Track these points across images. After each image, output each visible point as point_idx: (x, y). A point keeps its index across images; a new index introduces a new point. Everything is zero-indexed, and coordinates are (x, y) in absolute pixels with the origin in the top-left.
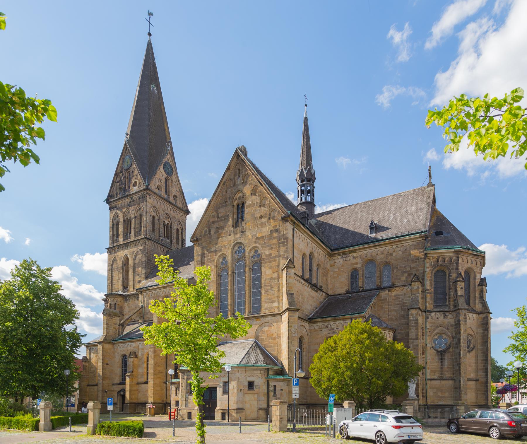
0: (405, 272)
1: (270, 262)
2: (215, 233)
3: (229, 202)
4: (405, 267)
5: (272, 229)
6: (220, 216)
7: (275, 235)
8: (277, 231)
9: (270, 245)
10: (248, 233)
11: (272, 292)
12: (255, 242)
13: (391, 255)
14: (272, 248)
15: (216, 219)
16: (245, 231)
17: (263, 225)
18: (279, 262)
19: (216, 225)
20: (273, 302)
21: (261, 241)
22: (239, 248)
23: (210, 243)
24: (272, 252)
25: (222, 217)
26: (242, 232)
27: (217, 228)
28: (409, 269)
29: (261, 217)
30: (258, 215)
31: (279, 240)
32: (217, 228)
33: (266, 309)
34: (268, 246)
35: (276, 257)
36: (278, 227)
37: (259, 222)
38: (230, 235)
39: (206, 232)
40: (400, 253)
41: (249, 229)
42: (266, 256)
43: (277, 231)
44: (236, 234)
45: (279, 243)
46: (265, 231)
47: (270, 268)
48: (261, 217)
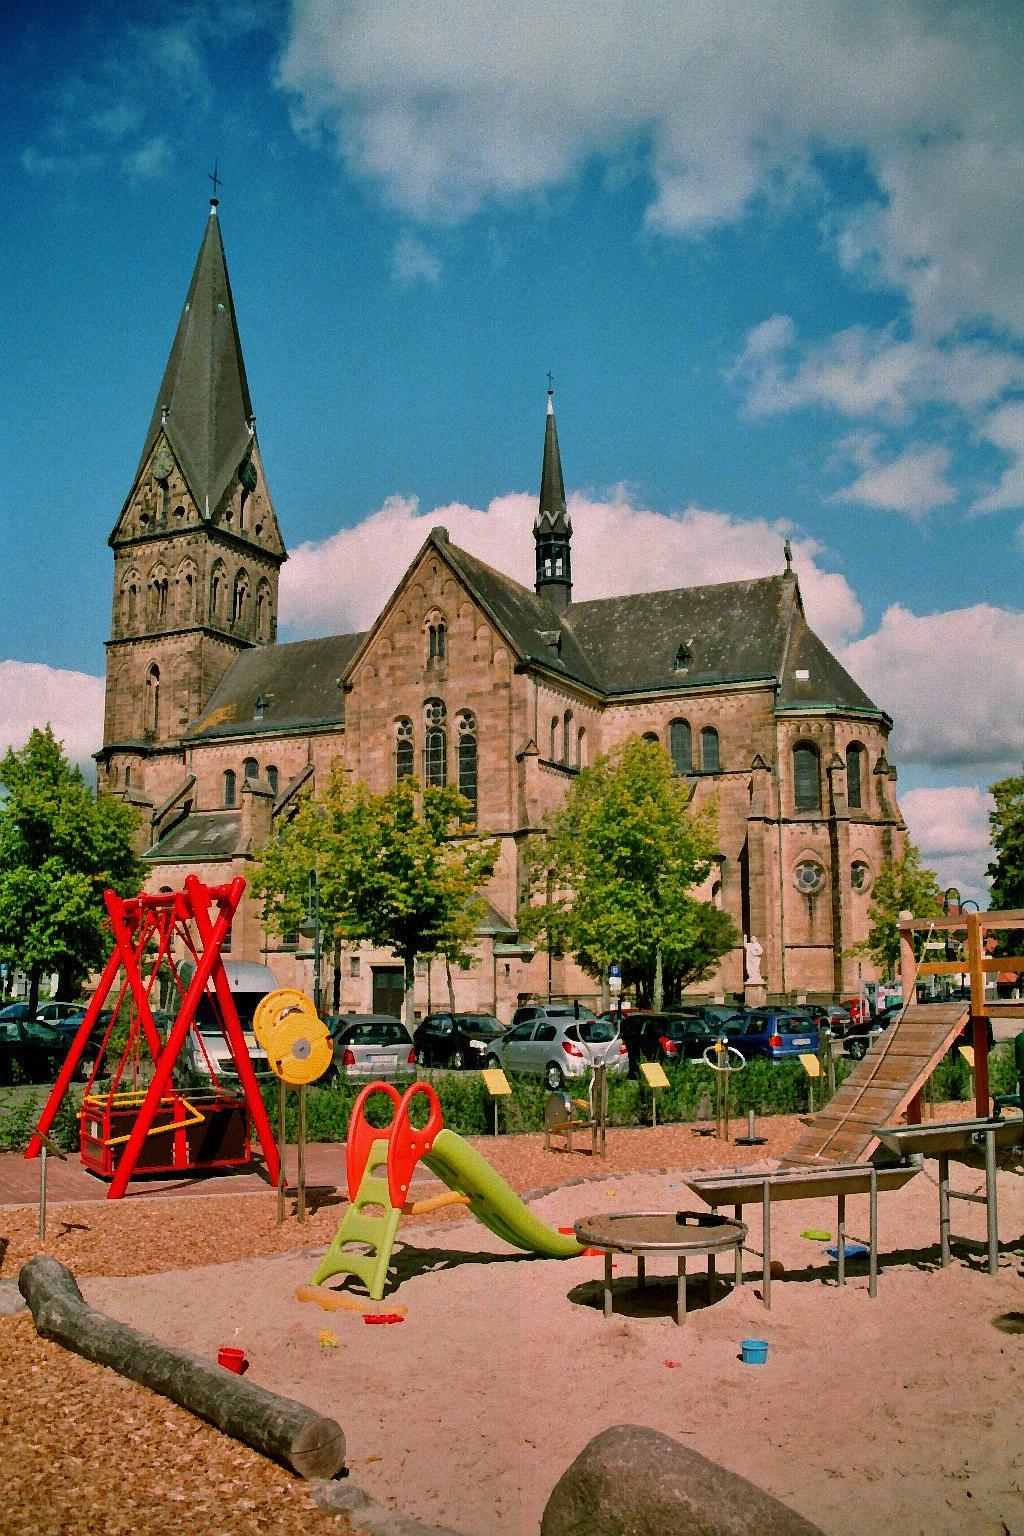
1: (493, 738)
2: (387, 675)
3: (415, 623)
5: (496, 681)
7: (503, 692)
8: (507, 686)
11: (497, 794)
17: (480, 673)
19: (389, 662)
23: (377, 693)
25: (401, 649)
27: (392, 668)
29: (475, 659)
30: (471, 654)
31: (511, 702)
32: (392, 668)
37: (473, 666)
42: (487, 727)
43: (507, 686)
46: (485, 684)
47: (494, 750)
48: (475, 659)
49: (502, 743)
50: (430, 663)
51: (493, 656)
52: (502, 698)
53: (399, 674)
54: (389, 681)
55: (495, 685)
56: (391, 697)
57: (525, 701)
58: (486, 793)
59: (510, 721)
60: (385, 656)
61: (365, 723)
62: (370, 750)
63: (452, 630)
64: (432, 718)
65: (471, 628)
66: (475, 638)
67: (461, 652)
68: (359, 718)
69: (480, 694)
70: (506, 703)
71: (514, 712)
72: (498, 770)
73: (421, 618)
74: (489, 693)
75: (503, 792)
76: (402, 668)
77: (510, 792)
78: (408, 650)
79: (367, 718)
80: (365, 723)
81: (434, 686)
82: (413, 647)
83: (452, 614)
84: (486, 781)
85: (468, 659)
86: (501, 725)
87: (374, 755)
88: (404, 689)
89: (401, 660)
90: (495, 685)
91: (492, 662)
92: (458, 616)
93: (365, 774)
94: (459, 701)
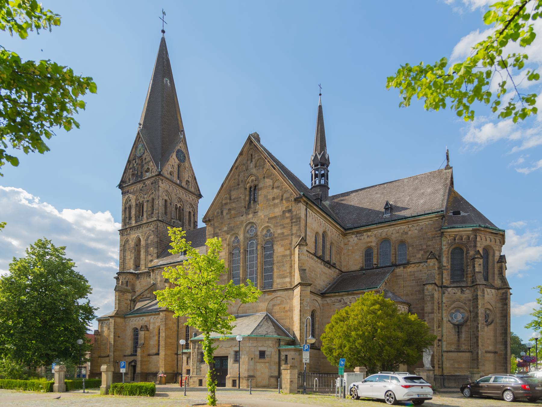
1: (282, 240)
2: (227, 214)
6: (232, 198)
7: (287, 215)
8: (290, 211)
9: (283, 225)
10: (260, 214)
14: (284, 227)
15: (229, 201)
16: (257, 212)
17: (275, 205)
18: (292, 240)
19: (228, 207)
23: (222, 223)
24: (284, 231)
25: (234, 199)
26: (255, 213)
27: (229, 210)
29: (274, 199)
32: (229, 210)
35: (288, 235)
36: (290, 208)
38: (242, 216)
42: (279, 234)
43: (290, 211)
45: (292, 223)
46: (278, 211)
47: (282, 246)
48: (274, 199)
54: (228, 216)
57: (300, 218)
59: (291, 230)
70: (288, 221)
76: (234, 209)
89: (234, 205)
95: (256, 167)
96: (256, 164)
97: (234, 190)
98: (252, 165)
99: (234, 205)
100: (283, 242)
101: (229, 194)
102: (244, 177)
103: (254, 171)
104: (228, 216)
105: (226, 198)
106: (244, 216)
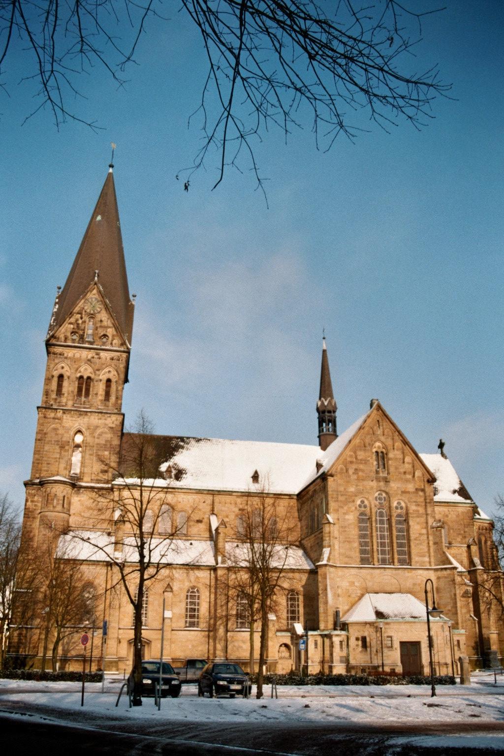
0: (459, 534)
1: (418, 517)
2: (353, 473)
3: (368, 448)
4: (459, 529)
5: (417, 487)
6: (359, 458)
7: (421, 493)
8: (423, 490)
11: (421, 547)
12: (401, 495)
13: (447, 516)
14: (419, 505)
16: (389, 482)
17: (407, 481)
19: (354, 466)
20: (424, 556)
21: (407, 495)
22: (379, 494)
23: (348, 482)
25: (361, 460)
27: (356, 469)
28: (462, 532)
29: (405, 473)
30: (402, 470)
31: (425, 499)
32: (356, 469)
33: (417, 562)
34: (415, 502)
35: (423, 514)
36: (423, 487)
37: (403, 476)
38: (372, 481)
39: (342, 469)
40: (455, 516)
41: (393, 481)
42: (413, 511)
43: (423, 490)
44: (380, 481)
45: (426, 502)
46: (411, 487)
47: (418, 523)
49: (423, 520)
50: (377, 472)
51: (414, 473)
52: (420, 496)
53: (360, 473)
54: (355, 477)
55: (417, 489)
56: (357, 486)
58: (415, 546)
60: (351, 462)
61: (341, 498)
62: (345, 514)
63: (391, 455)
64: (379, 501)
65: (401, 456)
66: (404, 462)
67: (396, 468)
68: (337, 495)
69: (409, 492)
70: (422, 499)
71: (428, 505)
72: (421, 534)
73: (371, 445)
74: (414, 492)
75: (424, 547)
76: (363, 471)
77: (429, 547)
78: (365, 462)
79: (342, 495)
80: (341, 498)
81: (382, 484)
82: (369, 460)
83: (390, 447)
84: (415, 539)
85: (400, 473)
86: (421, 510)
87: (347, 517)
88: (365, 483)
89: (361, 466)
90: (417, 489)
91: (414, 476)
92: (394, 449)
93: (342, 527)
94: (397, 494)
95: (383, 435)
96: (383, 432)
97: (360, 450)
98: (379, 432)
99: (361, 466)
100: (418, 520)
101: (355, 453)
102: (372, 441)
103: (383, 438)
104: (355, 477)
105: (351, 456)
106: (374, 481)
